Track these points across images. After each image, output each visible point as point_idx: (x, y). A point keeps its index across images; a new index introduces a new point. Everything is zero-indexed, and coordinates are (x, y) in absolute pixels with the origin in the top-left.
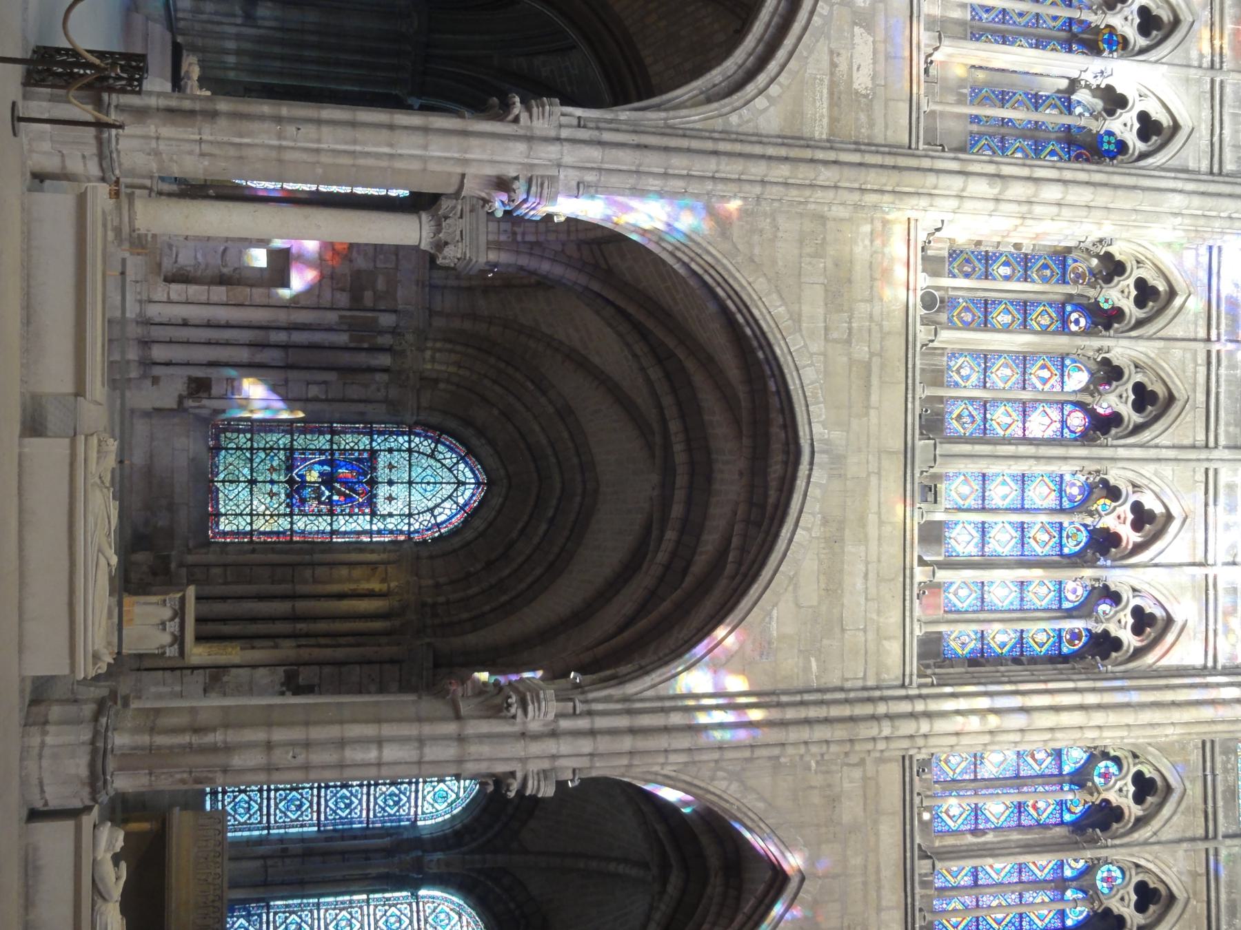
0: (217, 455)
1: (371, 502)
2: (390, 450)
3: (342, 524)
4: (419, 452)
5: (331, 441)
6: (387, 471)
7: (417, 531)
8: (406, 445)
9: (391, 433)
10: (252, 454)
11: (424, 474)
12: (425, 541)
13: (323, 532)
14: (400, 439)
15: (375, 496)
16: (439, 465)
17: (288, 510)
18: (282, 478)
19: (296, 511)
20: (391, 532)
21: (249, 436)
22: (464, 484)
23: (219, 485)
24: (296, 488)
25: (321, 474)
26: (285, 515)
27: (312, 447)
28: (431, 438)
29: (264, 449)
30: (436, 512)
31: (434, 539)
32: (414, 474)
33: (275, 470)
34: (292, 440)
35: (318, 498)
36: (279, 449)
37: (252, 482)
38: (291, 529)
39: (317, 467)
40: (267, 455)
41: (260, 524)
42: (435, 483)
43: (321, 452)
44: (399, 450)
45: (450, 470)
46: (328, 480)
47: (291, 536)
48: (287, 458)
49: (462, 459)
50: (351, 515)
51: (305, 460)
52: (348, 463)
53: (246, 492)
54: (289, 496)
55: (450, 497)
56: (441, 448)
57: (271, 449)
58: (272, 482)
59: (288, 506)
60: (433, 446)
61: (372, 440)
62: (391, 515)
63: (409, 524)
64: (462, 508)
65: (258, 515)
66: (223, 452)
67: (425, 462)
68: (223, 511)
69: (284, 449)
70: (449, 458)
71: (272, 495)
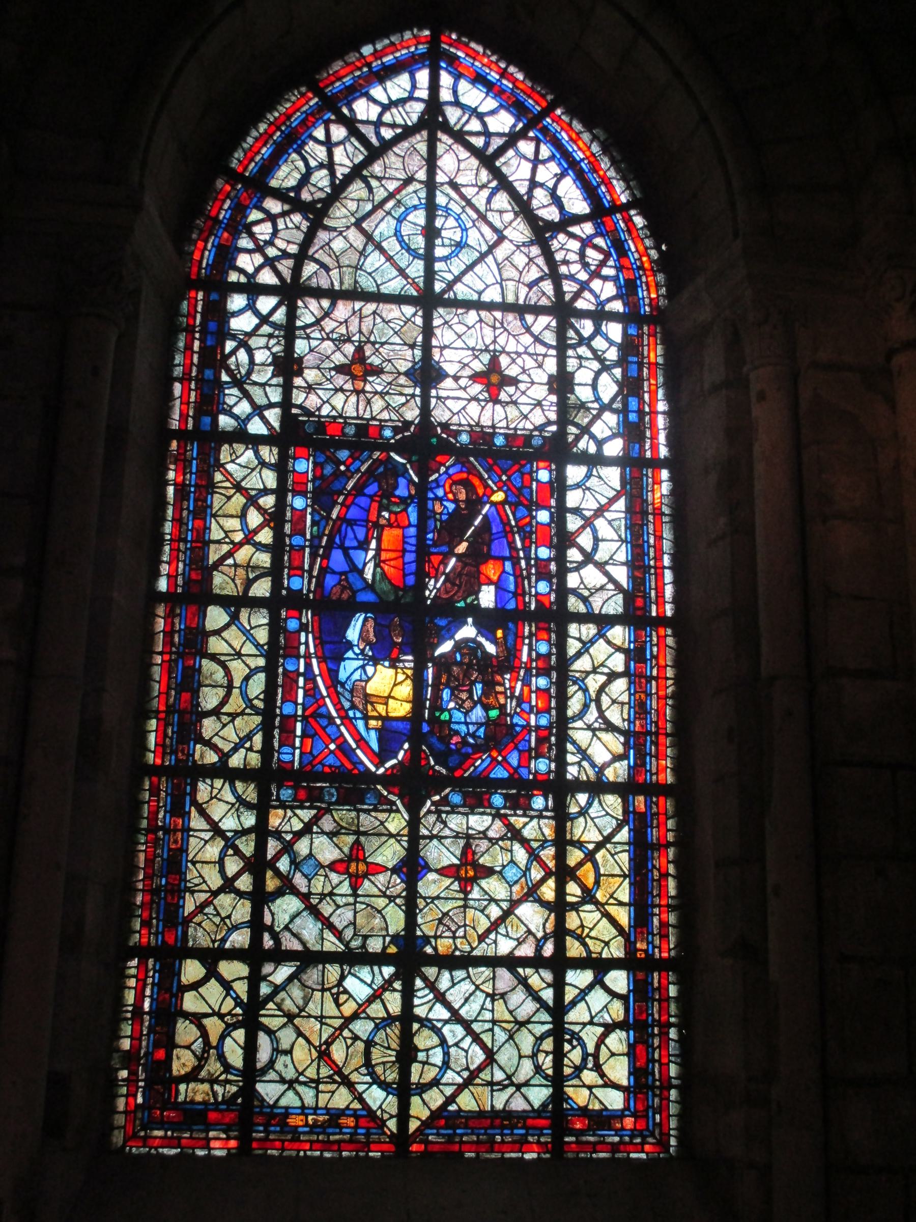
0: (277, 1116)
1: (511, 455)
2: (288, 366)
3: (600, 570)
4: (301, 258)
5: (236, 604)
6: (376, 384)
7: (628, 291)
8: (265, 304)
9: (214, 359)
10: (280, 956)
11: (392, 246)
12: (664, 264)
13: (635, 654)
14: (243, 323)
15: (482, 437)
16: (357, 189)
17: (538, 802)
18: (397, 823)
19: (542, 765)
20: (630, 387)
21: (192, 970)
22: (434, 105)
23: (419, 1110)
24: (430, 766)
25: (381, 651)
26: (562, 818)
27: (257, 685)
28: (240, 210)
29: (260, 899)
30: (551, 214)
31: (656, 230)
32: (395, 285)
33: (357, 853)
34: (222, 771)
35: (490, 670)
36: (262, 831)
37: (410, 957)
38: (623, 790)
39: (349, 668)
40: (287, 887)
41: (600, 930)
42: (431, 208)
43: (278, 649)
44: (289, 331)
45: (376, 152)
46: (407, 624)
47: (653, 790)
48: (312, 798)
49: (334, 106)
50: (564, 540)
51: (314, 716)
52: (333, 538)
53: (459, 988)
54: (476, 796)
55: (488, 160)
56: (286, 176)
57: (257, 865)
58: (412, 867)
59: (519, 803)
60: (274, 206)
61: (241, 436)
62: (562, 383)
63: (599, 316)
64: (534, 121)
65: (560, 933)
66: (268, 1090)
67: (339, 241)
68: (539, 1095)
69: (262, 809)
70: (329, 150)
71: (468, 871)
